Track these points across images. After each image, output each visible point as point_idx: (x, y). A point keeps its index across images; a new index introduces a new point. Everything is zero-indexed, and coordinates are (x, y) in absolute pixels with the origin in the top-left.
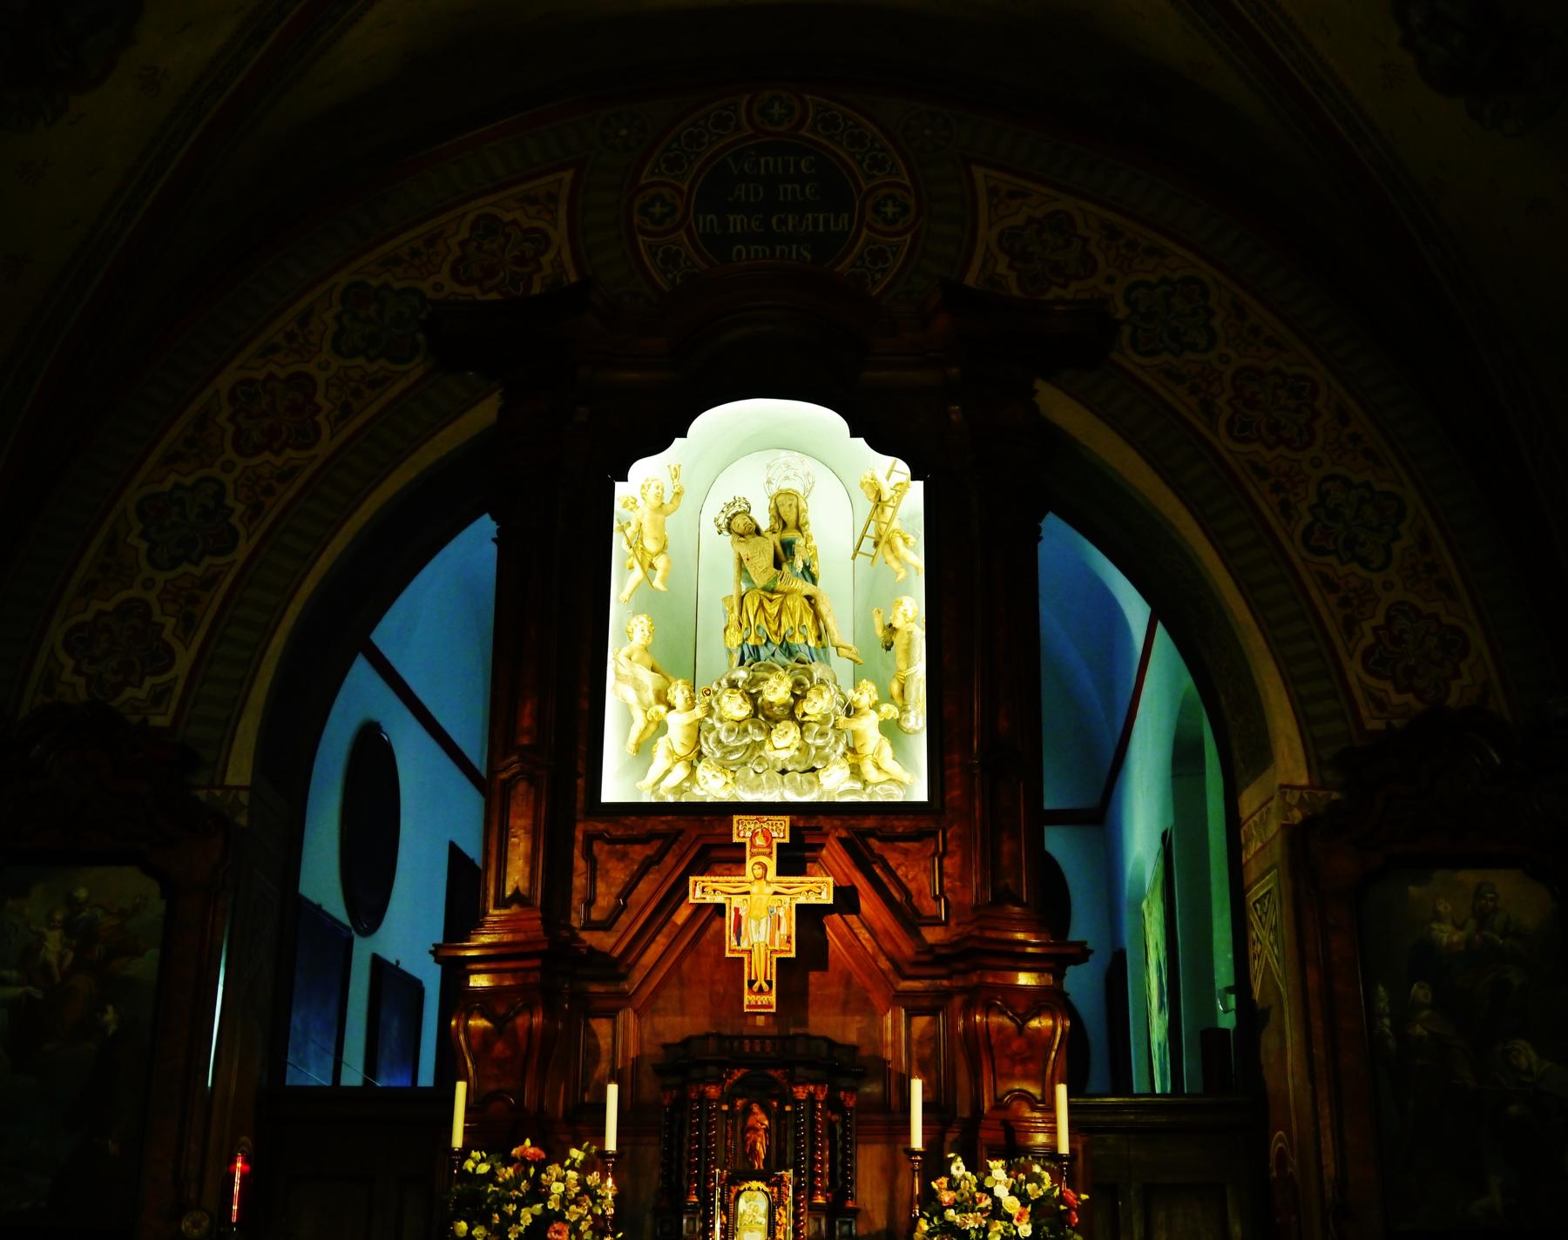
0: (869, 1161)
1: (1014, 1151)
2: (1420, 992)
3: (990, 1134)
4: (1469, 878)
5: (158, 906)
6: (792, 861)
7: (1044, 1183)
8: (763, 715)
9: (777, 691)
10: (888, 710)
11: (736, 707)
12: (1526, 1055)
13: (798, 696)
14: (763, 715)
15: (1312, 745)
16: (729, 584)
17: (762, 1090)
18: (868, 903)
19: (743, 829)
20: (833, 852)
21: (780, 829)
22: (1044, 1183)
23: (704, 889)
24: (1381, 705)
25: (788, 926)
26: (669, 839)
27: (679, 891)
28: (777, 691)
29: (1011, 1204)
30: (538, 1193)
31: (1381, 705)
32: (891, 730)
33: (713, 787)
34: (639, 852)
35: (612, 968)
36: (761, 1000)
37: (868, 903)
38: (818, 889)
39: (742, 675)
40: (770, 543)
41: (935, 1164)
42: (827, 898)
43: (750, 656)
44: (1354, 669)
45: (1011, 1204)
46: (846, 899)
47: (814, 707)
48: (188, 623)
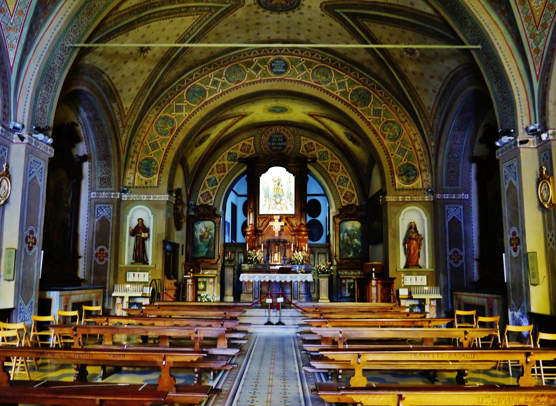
0: (288, 252)
1: (302, 250)
2: (346, 234)
3: (300, 249)
4: (352, 222)
5: (213, 225)
6: (280, 220)
7: (304, 254)
8: (277, 203)
9: (278, 200)
10: (291, 202)
11: (274, 202)
12: (356, 241)
13: (281, 201)
14: (277, 203)
15: (336, 207)
16: (273, 187)
17: (277, 245)
18: (288, 224)
19: (275, 217)
20: (284, 219)
21: (279, 217)
22: (304, 254)
23: (271, 224)
24: (344, 203)
25: (280, 227)
26: (267, 218)
27: (268, 223)
28: (278, 200)
29: (301, 256)
30: (255, 255)
31: (344, 203)
32: (291, 204)
33: (271, 212)
34: (264, 219)
35: (261, 231)
36: (277, 235)
37: (288, 224)
38: (282, 223)
39: (274, 198)
40: (277, 182)
41: (294, 252)
42: (283, 224)
43: (275, 196)
44: (342, 198)
45: (301, 256)
46: (286, 224)
47: (282, 202)
48: (214, 193)
